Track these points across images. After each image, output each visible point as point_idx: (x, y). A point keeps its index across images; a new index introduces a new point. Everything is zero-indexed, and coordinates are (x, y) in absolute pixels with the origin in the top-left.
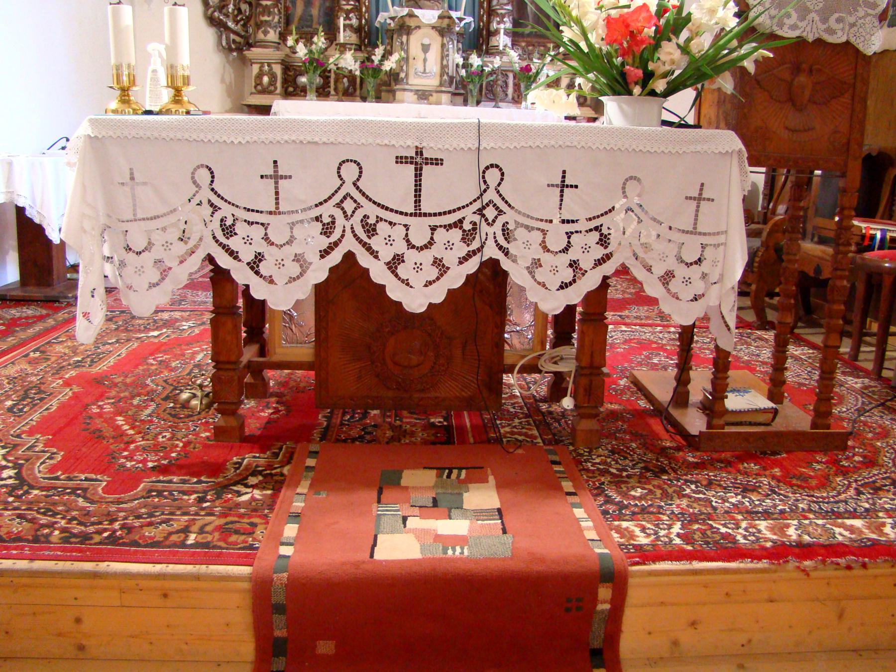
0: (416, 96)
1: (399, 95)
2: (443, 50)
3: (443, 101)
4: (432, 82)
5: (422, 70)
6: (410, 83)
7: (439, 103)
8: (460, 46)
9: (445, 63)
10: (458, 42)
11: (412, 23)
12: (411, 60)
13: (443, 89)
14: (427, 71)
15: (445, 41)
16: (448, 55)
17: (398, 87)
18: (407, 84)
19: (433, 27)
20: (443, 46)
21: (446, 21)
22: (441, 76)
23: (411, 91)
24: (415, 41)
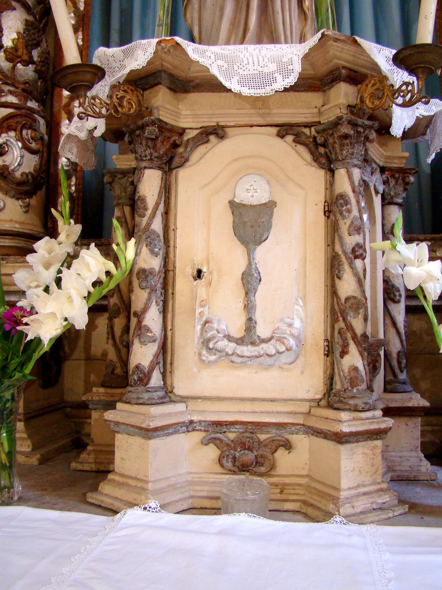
0: (212, 452)
1: (127, 452)
2: (333, 231)
3: (347, 482)
4: (286, 384)
5: (237, 330)
6: (181, 387)
7: (313, 504)
8: (396, 216)
9: (347, 287)
10: (386, 201)
11: (185, 113)
12: (183, 284)
13: (347, 422)
14: (263, 330)
15: (343, 185)
16: (358, 252)
17: (122, 413)
18: (168, 395)
19: (284, 130)
20: (333, 207)
21: (343, 95)
22: (333, 350)
23: (190, 427)
24: (199, 203)
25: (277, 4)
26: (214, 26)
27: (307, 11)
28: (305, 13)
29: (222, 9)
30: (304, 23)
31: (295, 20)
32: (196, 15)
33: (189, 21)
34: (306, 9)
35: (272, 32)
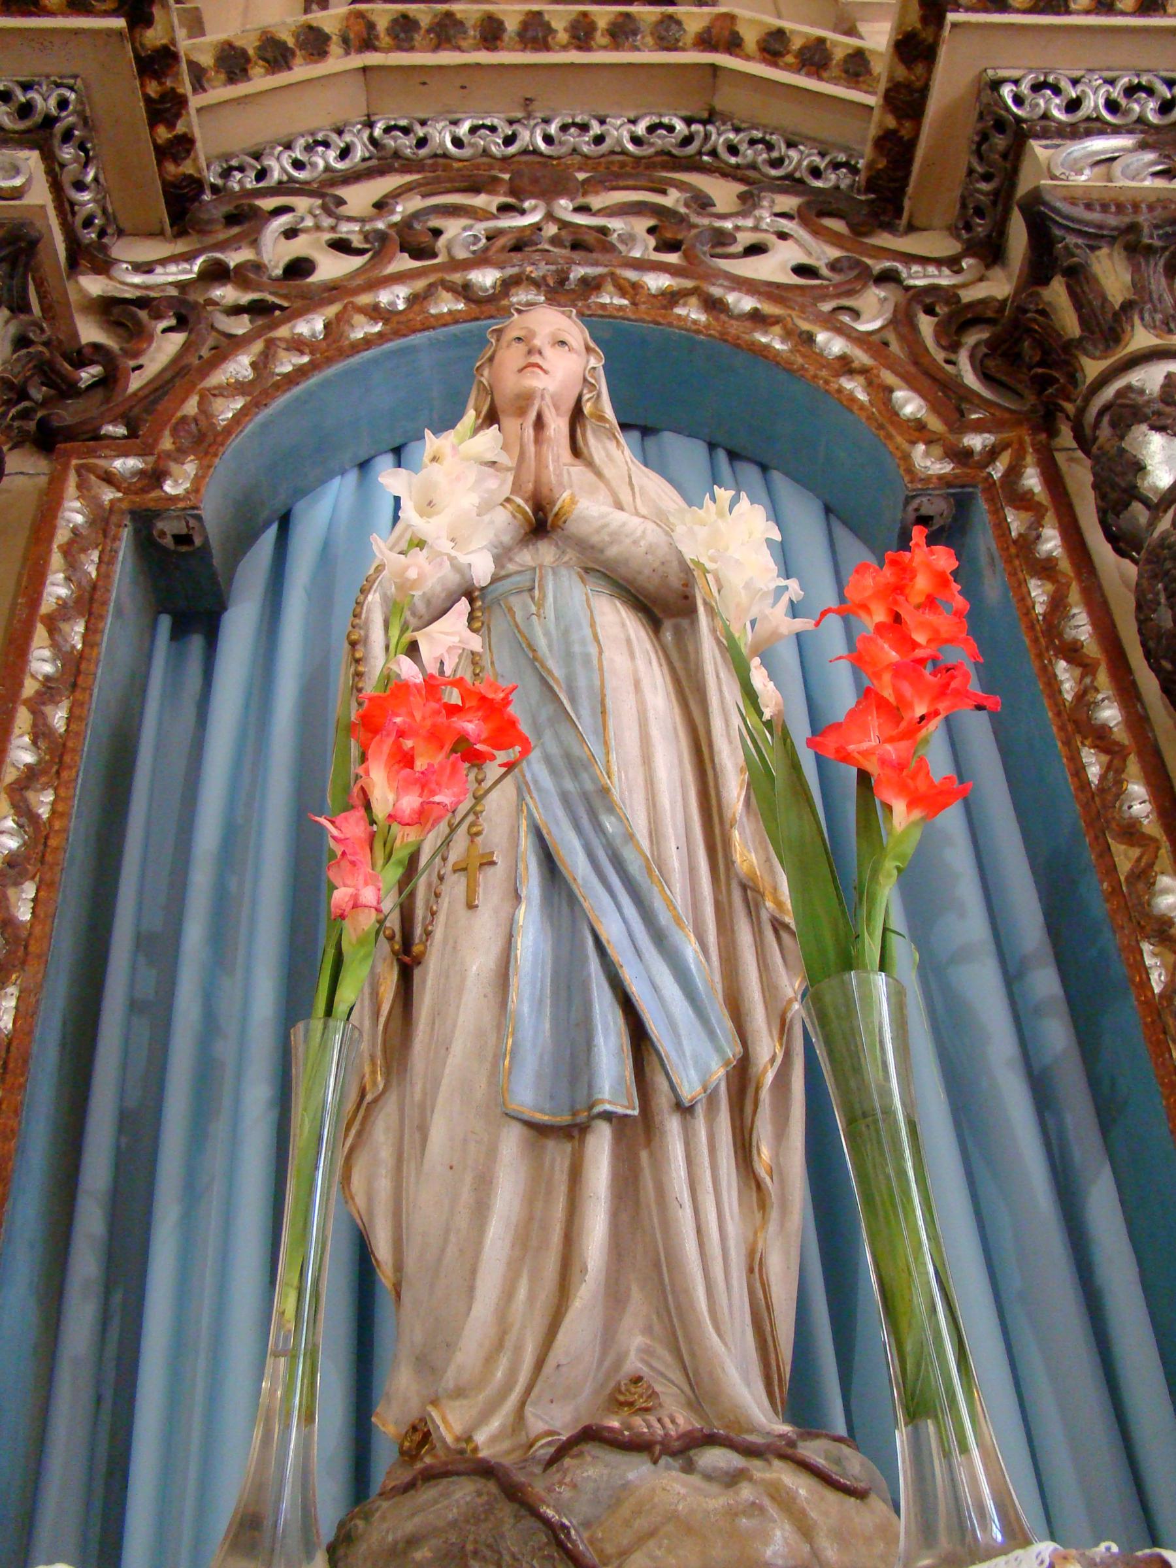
25: (674, 1175)
26: (453, 1238)
27: (768, 1179)
28: (759, 1186)
29: (484, 1184)
30: (758, 1215)
31: (732, 1218)
32: (384, 1185)
33: (360, 1200)
34: (762, 1173)
35: (657, 1265)
